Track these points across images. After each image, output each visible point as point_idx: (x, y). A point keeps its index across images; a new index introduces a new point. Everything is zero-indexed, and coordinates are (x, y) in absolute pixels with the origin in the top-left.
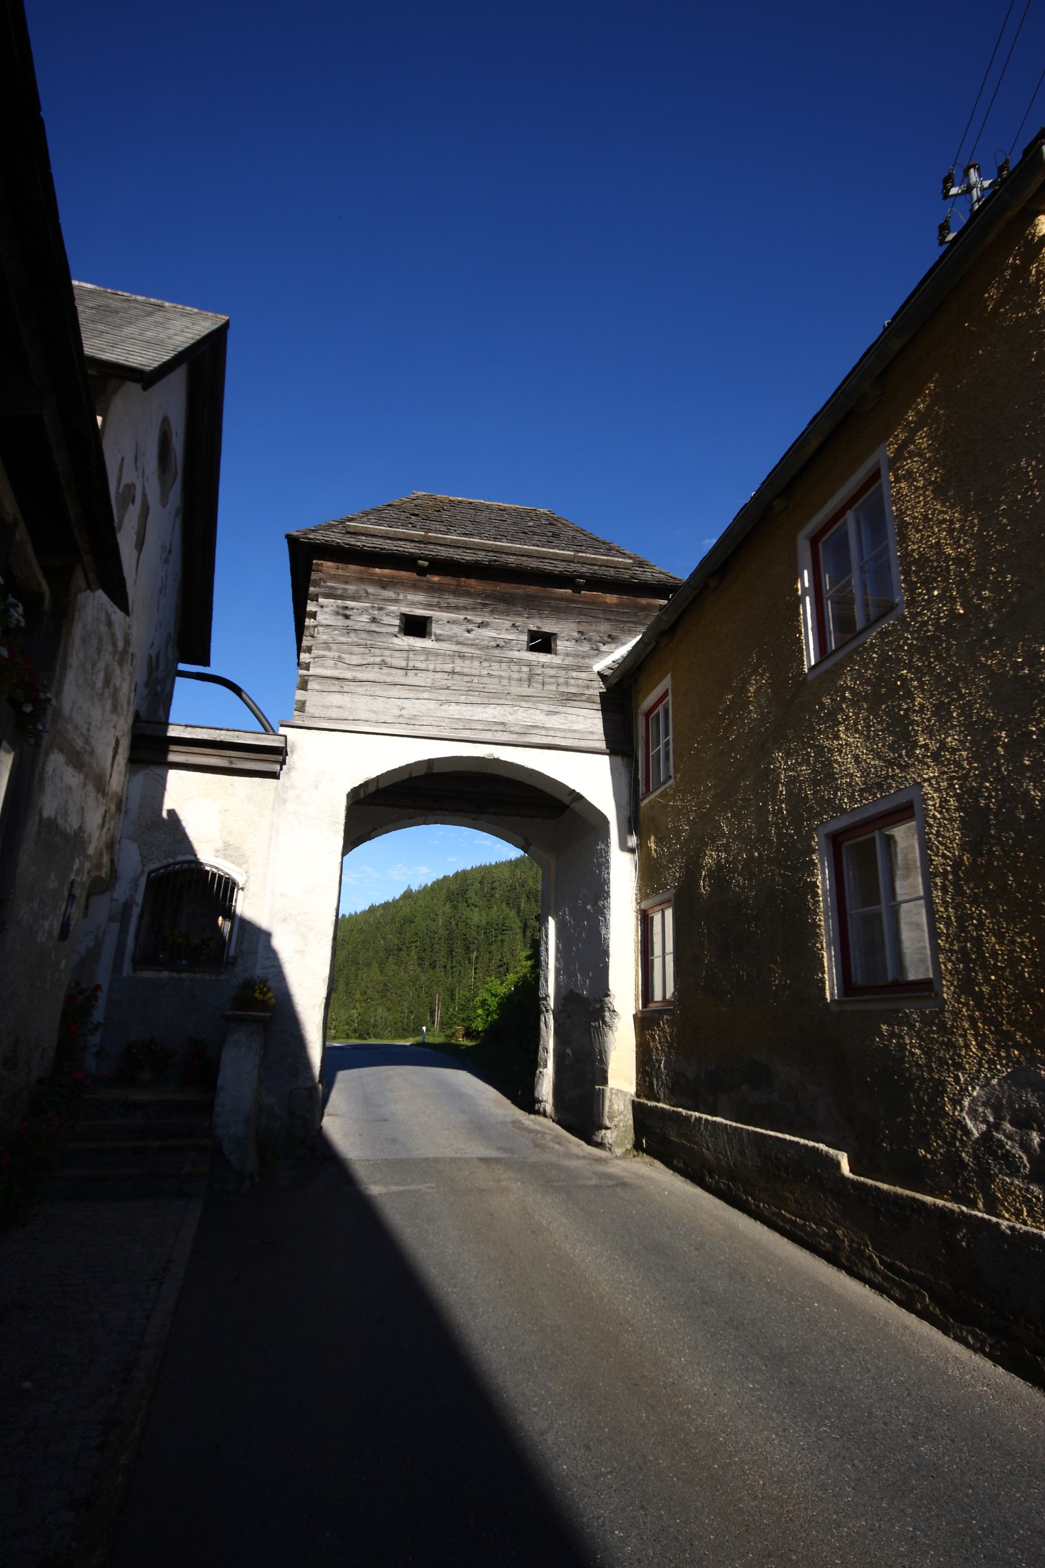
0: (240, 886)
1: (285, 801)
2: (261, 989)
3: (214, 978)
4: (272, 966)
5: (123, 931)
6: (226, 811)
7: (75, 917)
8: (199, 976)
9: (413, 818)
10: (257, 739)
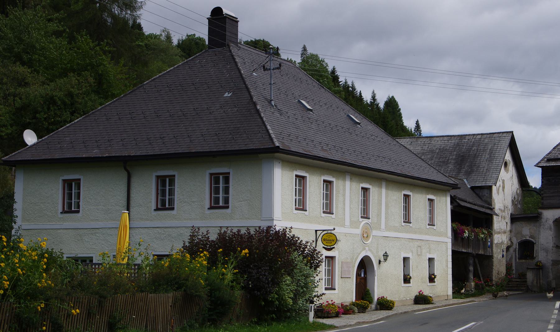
1: (541, 226)
5: (516, 253)
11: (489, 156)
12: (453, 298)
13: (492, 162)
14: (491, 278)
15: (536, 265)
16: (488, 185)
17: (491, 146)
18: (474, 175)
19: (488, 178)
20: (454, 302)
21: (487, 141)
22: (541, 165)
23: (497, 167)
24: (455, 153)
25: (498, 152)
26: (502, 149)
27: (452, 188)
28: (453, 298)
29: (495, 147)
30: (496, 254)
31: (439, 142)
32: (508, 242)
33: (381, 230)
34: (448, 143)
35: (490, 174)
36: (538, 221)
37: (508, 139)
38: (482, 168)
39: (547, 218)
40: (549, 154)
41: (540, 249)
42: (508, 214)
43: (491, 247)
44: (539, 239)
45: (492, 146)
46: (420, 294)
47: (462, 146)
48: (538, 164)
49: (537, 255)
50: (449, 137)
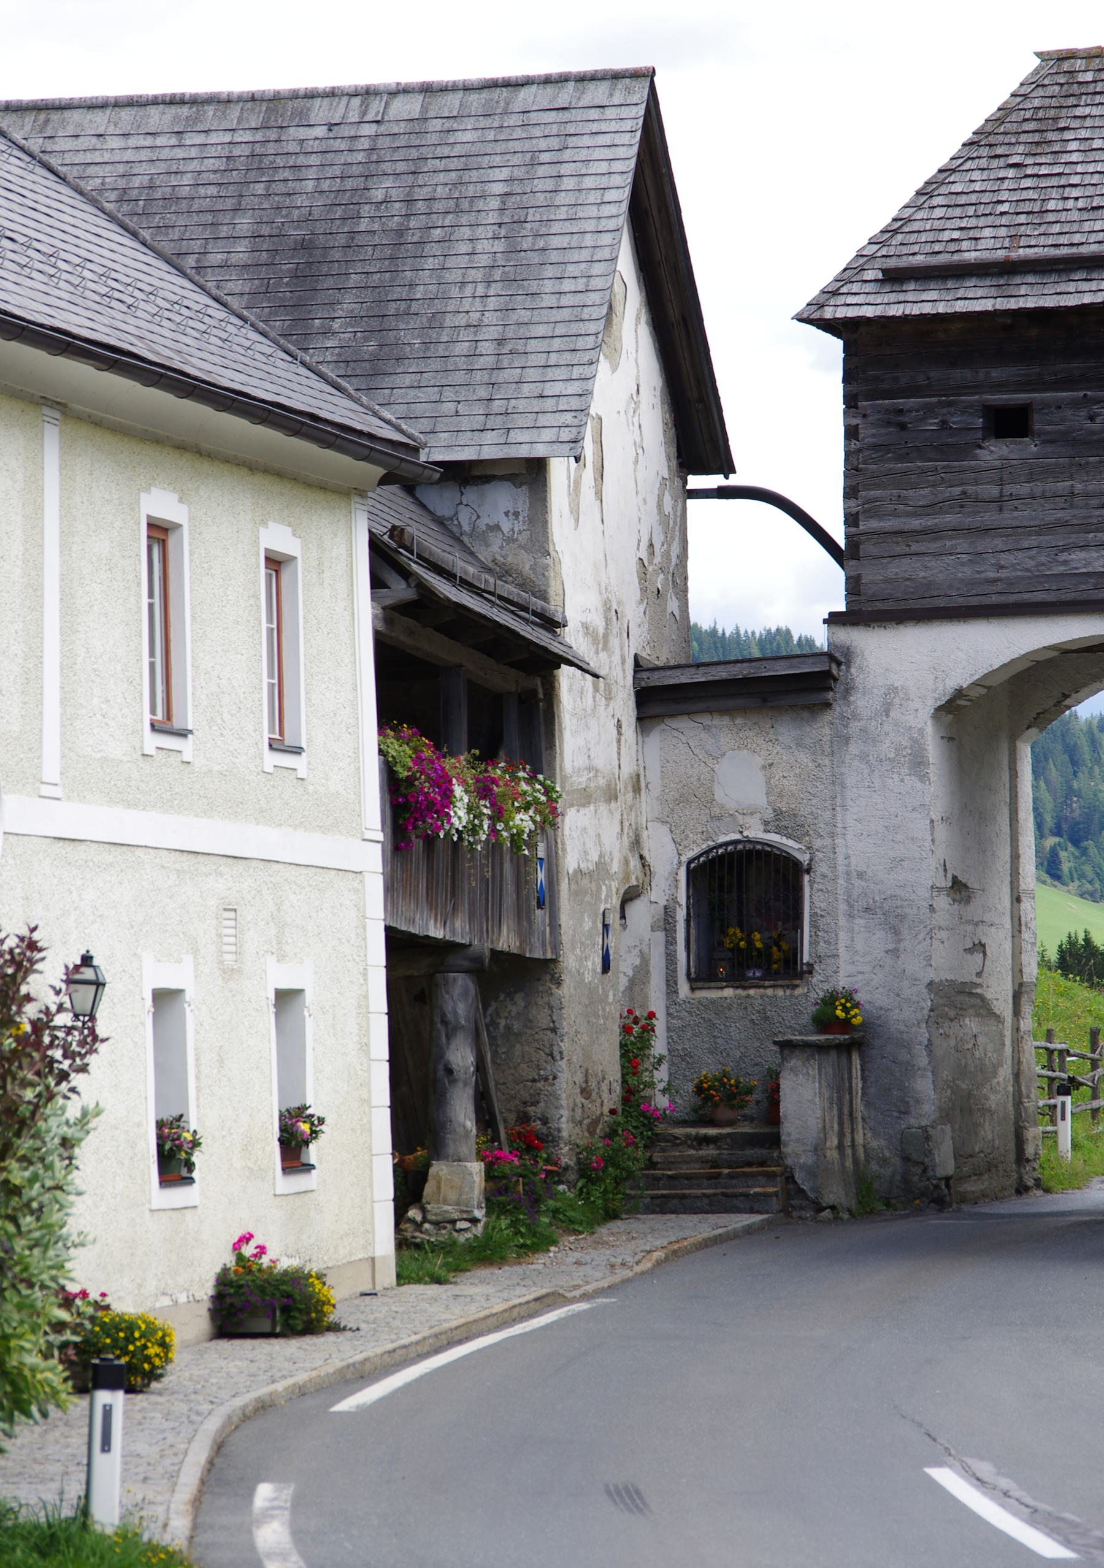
1: (847, 740)
2: (843, 1005)
3: (788, 992)
5: (670, 942)
6: (771, 765)
8: (770, 992)
10: (791, 667)
11: (499, 246)
12: (399, 1285)
13: (533, 287)
14: (545, 1121)
15: (825, 1021)
16: (524, 452)
17: (504, 174)
18: (408, 380)
19: (522, 405)
20: (474, 1312)
21: (468, 136)
22: (841, 313)
23: (574, 328)
24: (244, 223)
25: (562, 213)
26: (594, 197)
27: (380, 471)
28: (399, 1285)
29: (540, 185)
30: (574, 948)
31: (115, 143)
32: (626, 862)
33: (45, 790)
34: (180, 153)
35: (532, 374)
36: (828, 705)
37: (628, 125)
38: (464, 335)
39: (894, 690)
40: (890, 231)
41: (842, 907)
42: (623, 662)
43: (546, 899)
44: (832, 835)
45: (518, 173)
46: (240, 1258)
47: (287, 174)
48: (817, 304)
49: (822, 948)
50: (185, 111)
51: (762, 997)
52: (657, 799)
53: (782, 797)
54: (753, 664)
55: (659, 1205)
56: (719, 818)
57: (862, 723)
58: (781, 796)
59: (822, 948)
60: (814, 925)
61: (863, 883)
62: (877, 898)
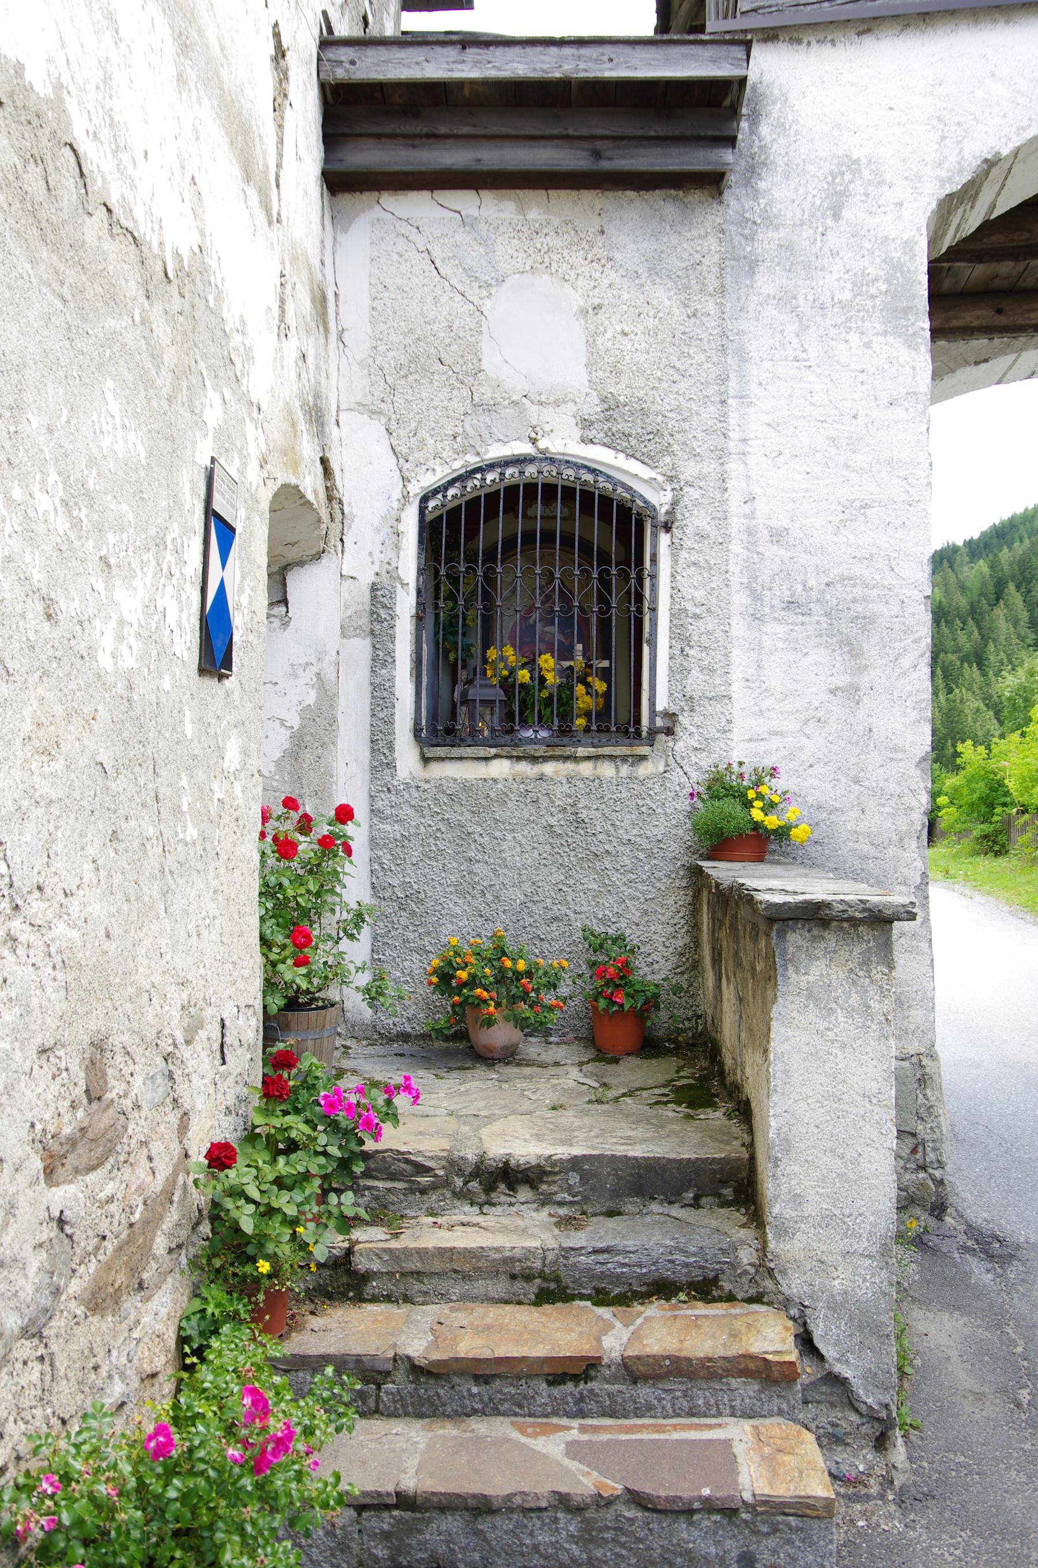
0: (662, 518)
1: (752, 265)
3: (625, 770)
4: (776, 733)
6: (597, 308)
7: (244, 600)
8: (586, 769)
9: (986, 361)
39: (853, 165)
41: (739, 600)
44: (721, 454)
49: (696, 681)
51: (569, 779)
52: (361, 363)
53: (619, 373)
54: (585, 51)
55: (386, 1536)
56: (491, 408)
57: (782, 233)
58: (616, 371)
59: (696, 681)
60: (681, 638)
61: (782, 552)
62: (812, 582)
